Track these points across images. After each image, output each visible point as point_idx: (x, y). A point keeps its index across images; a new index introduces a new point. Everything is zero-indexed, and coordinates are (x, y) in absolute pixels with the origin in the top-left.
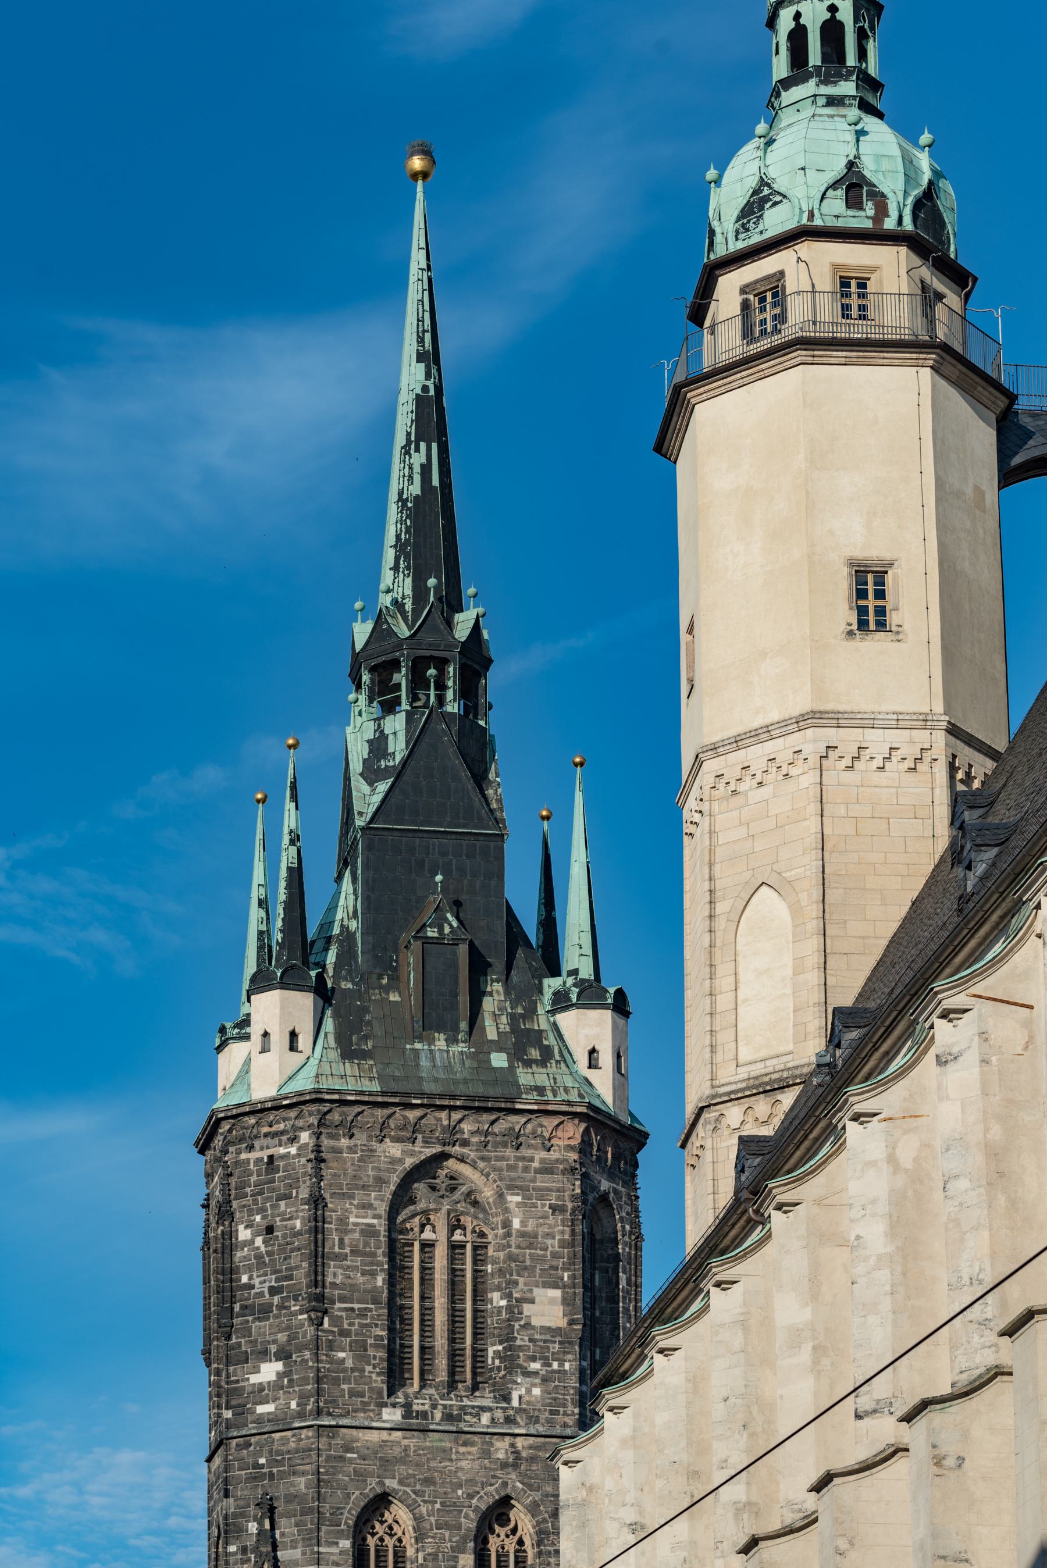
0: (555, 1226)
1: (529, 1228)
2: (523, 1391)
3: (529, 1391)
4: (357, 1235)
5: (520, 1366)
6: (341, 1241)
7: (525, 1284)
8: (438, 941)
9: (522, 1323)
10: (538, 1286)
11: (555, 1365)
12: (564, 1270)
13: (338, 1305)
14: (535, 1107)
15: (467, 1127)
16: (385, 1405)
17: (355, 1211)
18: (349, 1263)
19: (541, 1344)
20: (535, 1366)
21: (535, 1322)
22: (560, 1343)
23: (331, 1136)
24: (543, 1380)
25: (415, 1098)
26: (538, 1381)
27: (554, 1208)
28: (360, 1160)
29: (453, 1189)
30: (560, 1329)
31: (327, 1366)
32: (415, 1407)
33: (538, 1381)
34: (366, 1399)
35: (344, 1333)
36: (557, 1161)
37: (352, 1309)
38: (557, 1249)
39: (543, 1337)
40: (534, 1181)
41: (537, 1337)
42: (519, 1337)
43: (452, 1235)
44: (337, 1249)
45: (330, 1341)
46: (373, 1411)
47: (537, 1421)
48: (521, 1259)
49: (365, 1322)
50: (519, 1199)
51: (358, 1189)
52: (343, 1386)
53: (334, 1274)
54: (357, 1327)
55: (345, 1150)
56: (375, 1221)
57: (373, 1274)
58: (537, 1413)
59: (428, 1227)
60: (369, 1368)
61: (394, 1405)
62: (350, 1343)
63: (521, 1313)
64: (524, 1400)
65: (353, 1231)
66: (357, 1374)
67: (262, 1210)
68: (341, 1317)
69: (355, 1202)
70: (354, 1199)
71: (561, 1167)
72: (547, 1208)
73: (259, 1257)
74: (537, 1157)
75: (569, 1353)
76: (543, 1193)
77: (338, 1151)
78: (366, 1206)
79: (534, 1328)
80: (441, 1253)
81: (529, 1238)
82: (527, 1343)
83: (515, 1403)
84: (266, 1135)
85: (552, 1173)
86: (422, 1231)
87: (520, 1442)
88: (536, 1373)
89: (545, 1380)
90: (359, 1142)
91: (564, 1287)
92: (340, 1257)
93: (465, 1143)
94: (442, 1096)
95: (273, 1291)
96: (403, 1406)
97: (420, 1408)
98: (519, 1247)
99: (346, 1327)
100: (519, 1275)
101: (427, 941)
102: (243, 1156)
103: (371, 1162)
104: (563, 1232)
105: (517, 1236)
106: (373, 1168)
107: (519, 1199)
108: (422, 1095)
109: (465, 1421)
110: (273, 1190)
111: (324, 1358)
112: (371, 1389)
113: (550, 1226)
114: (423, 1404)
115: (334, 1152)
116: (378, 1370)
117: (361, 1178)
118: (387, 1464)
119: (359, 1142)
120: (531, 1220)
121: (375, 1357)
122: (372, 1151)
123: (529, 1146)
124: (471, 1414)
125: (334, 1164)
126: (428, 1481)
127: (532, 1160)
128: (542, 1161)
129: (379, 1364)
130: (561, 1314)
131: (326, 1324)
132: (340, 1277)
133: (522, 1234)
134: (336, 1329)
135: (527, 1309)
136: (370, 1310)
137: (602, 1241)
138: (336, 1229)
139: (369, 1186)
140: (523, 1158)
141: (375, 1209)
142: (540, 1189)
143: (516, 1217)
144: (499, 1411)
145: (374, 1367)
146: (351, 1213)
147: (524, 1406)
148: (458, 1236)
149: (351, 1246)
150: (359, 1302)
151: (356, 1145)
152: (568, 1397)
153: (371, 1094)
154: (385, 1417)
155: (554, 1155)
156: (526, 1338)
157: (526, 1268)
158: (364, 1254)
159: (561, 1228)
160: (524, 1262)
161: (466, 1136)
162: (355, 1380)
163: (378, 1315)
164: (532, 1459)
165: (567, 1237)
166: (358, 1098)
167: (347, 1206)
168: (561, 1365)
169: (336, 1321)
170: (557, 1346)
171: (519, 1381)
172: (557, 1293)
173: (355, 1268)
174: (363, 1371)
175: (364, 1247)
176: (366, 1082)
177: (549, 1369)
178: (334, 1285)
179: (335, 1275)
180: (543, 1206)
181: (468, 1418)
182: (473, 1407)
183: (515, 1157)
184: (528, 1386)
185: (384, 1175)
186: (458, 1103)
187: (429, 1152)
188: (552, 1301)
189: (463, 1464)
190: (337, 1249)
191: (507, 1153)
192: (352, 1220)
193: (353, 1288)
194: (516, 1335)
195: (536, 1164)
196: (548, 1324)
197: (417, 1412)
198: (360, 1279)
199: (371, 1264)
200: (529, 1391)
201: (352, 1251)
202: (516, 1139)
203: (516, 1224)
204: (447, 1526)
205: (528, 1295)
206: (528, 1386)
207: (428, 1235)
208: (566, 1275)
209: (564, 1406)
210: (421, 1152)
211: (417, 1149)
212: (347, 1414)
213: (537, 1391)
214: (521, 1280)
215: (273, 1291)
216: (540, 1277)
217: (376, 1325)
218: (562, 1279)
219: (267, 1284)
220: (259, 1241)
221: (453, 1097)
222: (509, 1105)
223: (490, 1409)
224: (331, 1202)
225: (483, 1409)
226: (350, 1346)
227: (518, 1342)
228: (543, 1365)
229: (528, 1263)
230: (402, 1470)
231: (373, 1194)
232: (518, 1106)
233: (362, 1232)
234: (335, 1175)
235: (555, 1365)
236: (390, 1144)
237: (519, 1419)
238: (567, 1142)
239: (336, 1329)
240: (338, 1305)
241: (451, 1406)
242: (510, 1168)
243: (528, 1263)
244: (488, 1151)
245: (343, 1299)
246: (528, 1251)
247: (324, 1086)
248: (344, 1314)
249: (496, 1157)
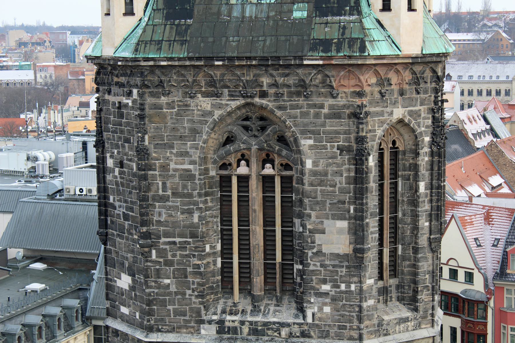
0: (342, 165)
1: (320, 168)
2: (316, 309)
3: (321, 309)
4: (177, 180)
5: (313, 288)
6: (164, 184)
7: (317, 217)
9: (315, 250)
10: (328, 219)
11: (343, 287)
12: (349, 203)
13: (163, 240)
14: (321, 62)
15: (265, 81)
16: (202, 322)
17: (174, 158)
18: (170, 204)
19: (331, 268)
20: (326, 288)
21: (325, 249)
22: (348, 267)
23: (152, 95)
24: (332, 300)
25: (217, 60)
26: (328, 300)
27: (341, 149)
28: (177, 114)
29: (263, 129)
30: (347, 255)
31: (156, 291)
32: (227, 324)
33: (328, 300)
34: (187, 318)
35: (169, 263)
36: (344, 106)
37: (174, 243)
38: (344, 185)
39: (333, 263)
40: (324, 125)
41: (327, 262)
42: (312, 263)
43: (263, 168)
44: (161, 192)
45: (158, 270)
46: (193, 327)
48: (313, 195)
49: (185, 253)
50: (311, 142)
51: (176, 140)
52: (168, 307)
53: (160, 213)
54: (178, 258)
55: (165, 106)
56: (191, 167)
57: (190, 212)
58: (327, 328)
59: (243, 162)
60: (188, 292)
61: (210, 322)
62: (174, 271)
63: (313, 242)
64: (318, 315)
65: (173, 176)
66: (180, 297)
67: (117, 147)
68: (166, 249)
69: (175, 151)
70: (173, 148)
71: (348, 111)
72: (335, 150)
73: (117, 184)
74: (326, 104)
75: (354, 276)
76: (332, 137)
77: (157, 107)
78: (184, 154)
79: (324, 255)
80: (255, 185)
81: (320, 177)
82: (319, 268)
83: (309, 320)
84: (117, 84)
85: (340, 117)
86: (238, 166)
88: (326, 294)
89: (334, 299)
90: (176, 99)
91: (350, 218)
92: (164, 199)
93: (263, 95)
94: (239, 58)
95: (126, 217)
96: (217, 323)
97: (231, 324)
98: (311, 185)
99: (170, 258)
100: (312, 209)
102: (107, 97)
103: (187, 116)
104: (349, 170)
105: (310, 175)
106: (188, 120)
107: (311, 142)
108: (222, 59)
109: (268, 336)
110: (122, 132)
111: (153, 284)
112: (191, 309)
113: (338, 165)
114: (233, 321)
115: (155, 109)
116: (196, 293)
117: (178, 130)
119: (176, 99)
120: (322, 161)
121: (193, 283)
122: (186, 105)
123: (320, 94)
124: (272, 329)
125: (157, 119)
127: (322, 107)
128: (331, 107)
129: (197, 288)
130: (347, 242)
131: (154, 257)
132: (164, 216)
133: (314, 173)
134: (161, 260)
135: (319, 238)
136: (189, 243)
137: (404, 153)
138: (160, 175)
139: (185, 136)
140: (315, 106)
141: (191, 156)
142: (330, 132)
143: (309, 158)
144: (296, 326)
145: (193, 291)
146: (171, 160)
147: (317, 322)
148: (268, 170)
149: (172, 189)
150: (180, 236)
151: (173, 102)
152: (354, 314)
153: (180, 59)
154: (203, 332)
155: (341, 101)
156: (318, 264)
157: (318, 203)
158: (183, 196)
159: (347, 166)
160: (316, 197)
161: (265, 89)
162: (179, 302)
163: (196, 247)
165: (353, 174)
166: (170, 63)
167: (168, 154)
168: (348, 286)
169: (161, 253)
170: (344, 270)
171: (312, 300)
172: (343, 224)
173: (176, 208)
174: (185, 294)
175: (183, 189)
176: (177, 46)
177: (338, 290)
178: (159, 222)
179: (160, 214)
180: (332, 147)
181: (270, 332)
182: (274, 323)
183: (308, 104)
184: (320, 305)
185: (197, 126)
186: (254, 63)
187: (234, 104)
188: (340, 231)
190: (161, 192)
191: (301, 102)
192: (172, 166)
193: (175, 225)
194: (309, 261)
195: (326, 111)
196: (336, 252)
197: (229, 327)
198: (180, 217)
199: (190, 203)
200: (321, 309)
201: (173, 193)
203: (309, 164)
205: (320, 227)
206: (320, 305)
207: (243, 170)
208: (352, 208)
209: (351, 321)
210: (227, 105)
211: (223, 102)
212: (172, 330)
213: (327, 309)
214: (313, 214)
215: (126, 217)
216: (330, 210)
217: (194, 256)
218: (349, 211)
219: (121, 209)
220: (117, 170)
221: (249, 58)
222: (298, 62)
223: (289, 325)
224: (155, 152)
225: (283, 325)
226: (174, 274)
227: (311, 268)
228: (332, 287)
229: (319, 199)
231: (189, 143)
232: (305, 62)
233: (181, 177)
234: (157, 128)
235: (343, 287)
236: (201, 99)
237: (312, 334)
238: (352, 90)
239: (161, 260)
240: (163, 240)
241: (256, 322)
242: (304, 115)
243: (319, 199)
244: (284, 101)
245: (166, 235)
246: (319, 188)
247: (140, 56)
248: (168, 247)
249: (291, 105)
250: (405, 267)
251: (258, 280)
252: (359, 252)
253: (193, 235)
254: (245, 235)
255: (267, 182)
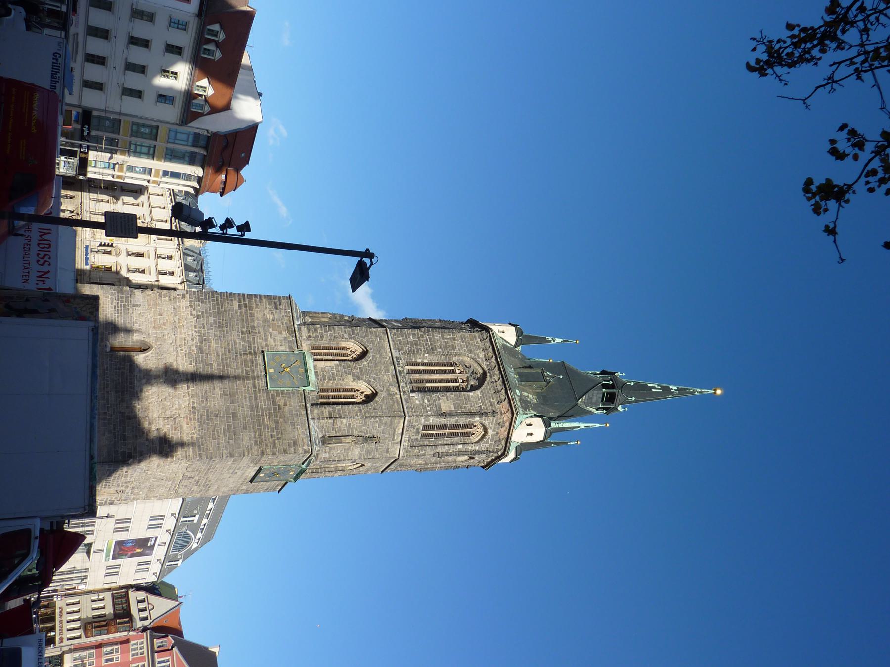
8: (544, 376)
47: (407, 402)
81: (468, 399)
83: (411, 395)
87: (398, 396)
92: (443, 338)
93: (491, 377)
101: (543, 373)
118: (379, 351)
126: (376, 365)
155: (497, 406)
164: (393, 400)
188: (450, 407)
189: (385, 377)
202: (497, 392)
204: (361, 371)
207: (458, 371)
213: (417, 402)
230: (378, 356)
250: (426, 442)
251: (417, 376)
252: (444, 415)
253: (432, 349)
254: (432, 372)
255: (456, 381)
